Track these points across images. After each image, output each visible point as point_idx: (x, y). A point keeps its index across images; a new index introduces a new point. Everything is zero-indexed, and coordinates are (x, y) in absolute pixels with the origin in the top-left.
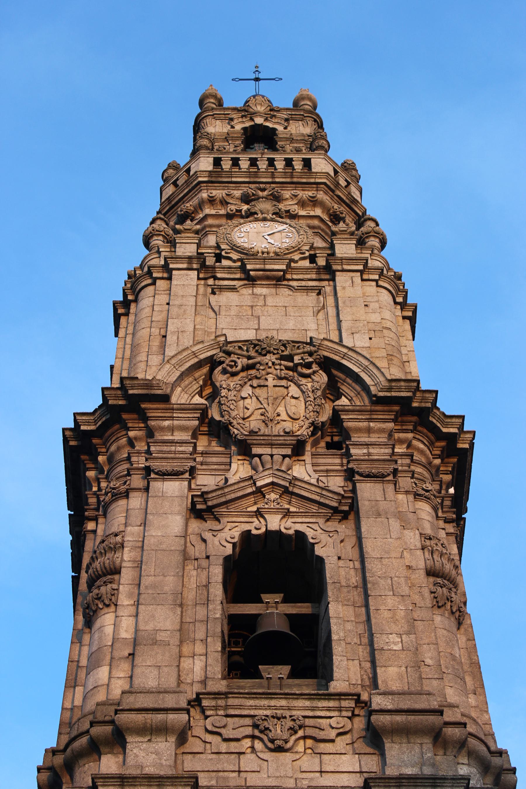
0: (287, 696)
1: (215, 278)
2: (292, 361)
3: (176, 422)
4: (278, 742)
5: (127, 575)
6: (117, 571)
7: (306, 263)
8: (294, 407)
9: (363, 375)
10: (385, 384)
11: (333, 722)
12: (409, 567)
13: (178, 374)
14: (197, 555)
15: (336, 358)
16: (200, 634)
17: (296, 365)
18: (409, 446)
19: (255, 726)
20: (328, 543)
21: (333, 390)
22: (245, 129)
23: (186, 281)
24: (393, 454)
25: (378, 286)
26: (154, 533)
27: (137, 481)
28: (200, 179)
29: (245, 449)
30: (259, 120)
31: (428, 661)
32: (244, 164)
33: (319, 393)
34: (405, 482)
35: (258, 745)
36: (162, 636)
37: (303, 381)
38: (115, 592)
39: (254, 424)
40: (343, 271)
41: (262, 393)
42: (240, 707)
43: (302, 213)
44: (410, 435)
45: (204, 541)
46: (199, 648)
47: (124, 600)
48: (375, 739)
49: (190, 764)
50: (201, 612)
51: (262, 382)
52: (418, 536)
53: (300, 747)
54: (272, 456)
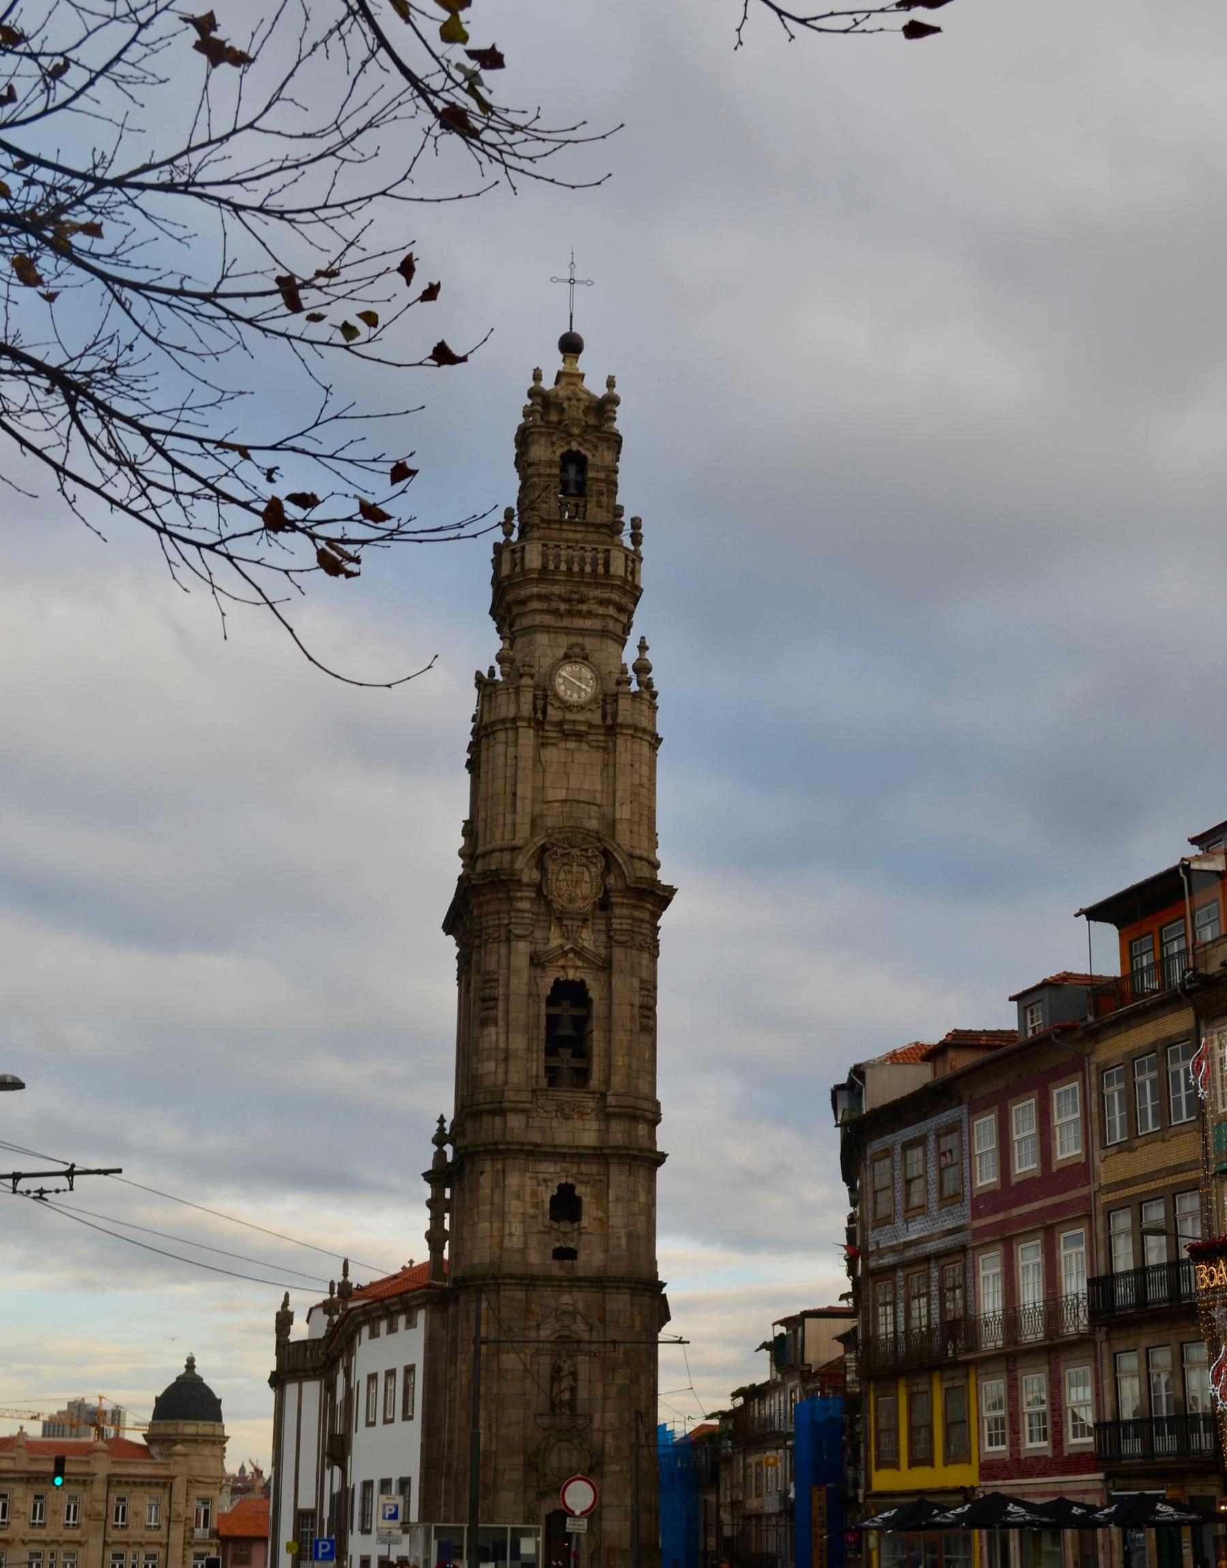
1: (543, 729)
6: (496, 999)
15: (610, 849)
16: (535, 1048)
21: (607, 870)
22: (563, 456)
23: (527, 738)
28: (533, 576)
29: (559, 919)
30: (575, 446)
36: (520, 1053)
41: (569, 877)
43: (601, 611)
46: (535, 1057)
47: (501, 1023)
48: (606, 1116)
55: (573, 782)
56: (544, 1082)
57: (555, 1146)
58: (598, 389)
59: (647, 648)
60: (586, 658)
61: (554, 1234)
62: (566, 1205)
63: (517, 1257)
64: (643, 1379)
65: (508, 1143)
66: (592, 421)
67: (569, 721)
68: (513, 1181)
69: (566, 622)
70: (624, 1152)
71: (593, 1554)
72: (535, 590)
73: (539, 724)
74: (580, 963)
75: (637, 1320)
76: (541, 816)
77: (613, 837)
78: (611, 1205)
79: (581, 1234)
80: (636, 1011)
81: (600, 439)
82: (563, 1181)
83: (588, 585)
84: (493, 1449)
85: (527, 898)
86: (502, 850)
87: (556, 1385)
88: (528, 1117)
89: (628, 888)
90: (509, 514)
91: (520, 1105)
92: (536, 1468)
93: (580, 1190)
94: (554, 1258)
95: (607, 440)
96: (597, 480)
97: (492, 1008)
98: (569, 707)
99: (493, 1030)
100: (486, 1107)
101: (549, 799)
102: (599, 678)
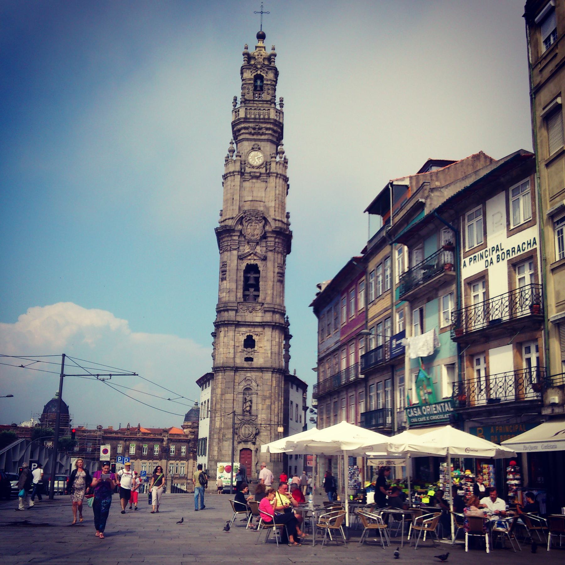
5: (227, 273)
22: (255, 76)
23: (238, 178)
26: (232, 265)
27: (229, 248)
29: (248, 243)
30: (259, 72)
34: (277, 249)
43: (267, 132)
47: (227, 279)
55: (255, 194)
56: (242, 300)
58: (269, 52)
59: (283, 145)
60: (260, 149)
61: (245, 352)
62: (250, 343)
63: (232, 361)
64: (276, 403)
65: (228, 321)
66: (266, 63)
67: (253, 172)
68: (231, 334)
69: (255, 137)
71: (257, 464)
72: (243, 125)
73: (242, 173)
74: (256, 258)
75: (274, 382)
76: (243, 206)
77: (268, 213)
80: (276, 274)
81: (268, 69)
82: (248, 334)
83: (262, 123)
86: (229, 219)
90: (235, 99)
92: (237, 434)
93: (254, 337)
95: (271, 69)
96: (267, 84)
97: (225, 274)
98: (253, 167)
99: (225, 282)
100: (222, 309)
101: (246, 200)
102: (264, 156)
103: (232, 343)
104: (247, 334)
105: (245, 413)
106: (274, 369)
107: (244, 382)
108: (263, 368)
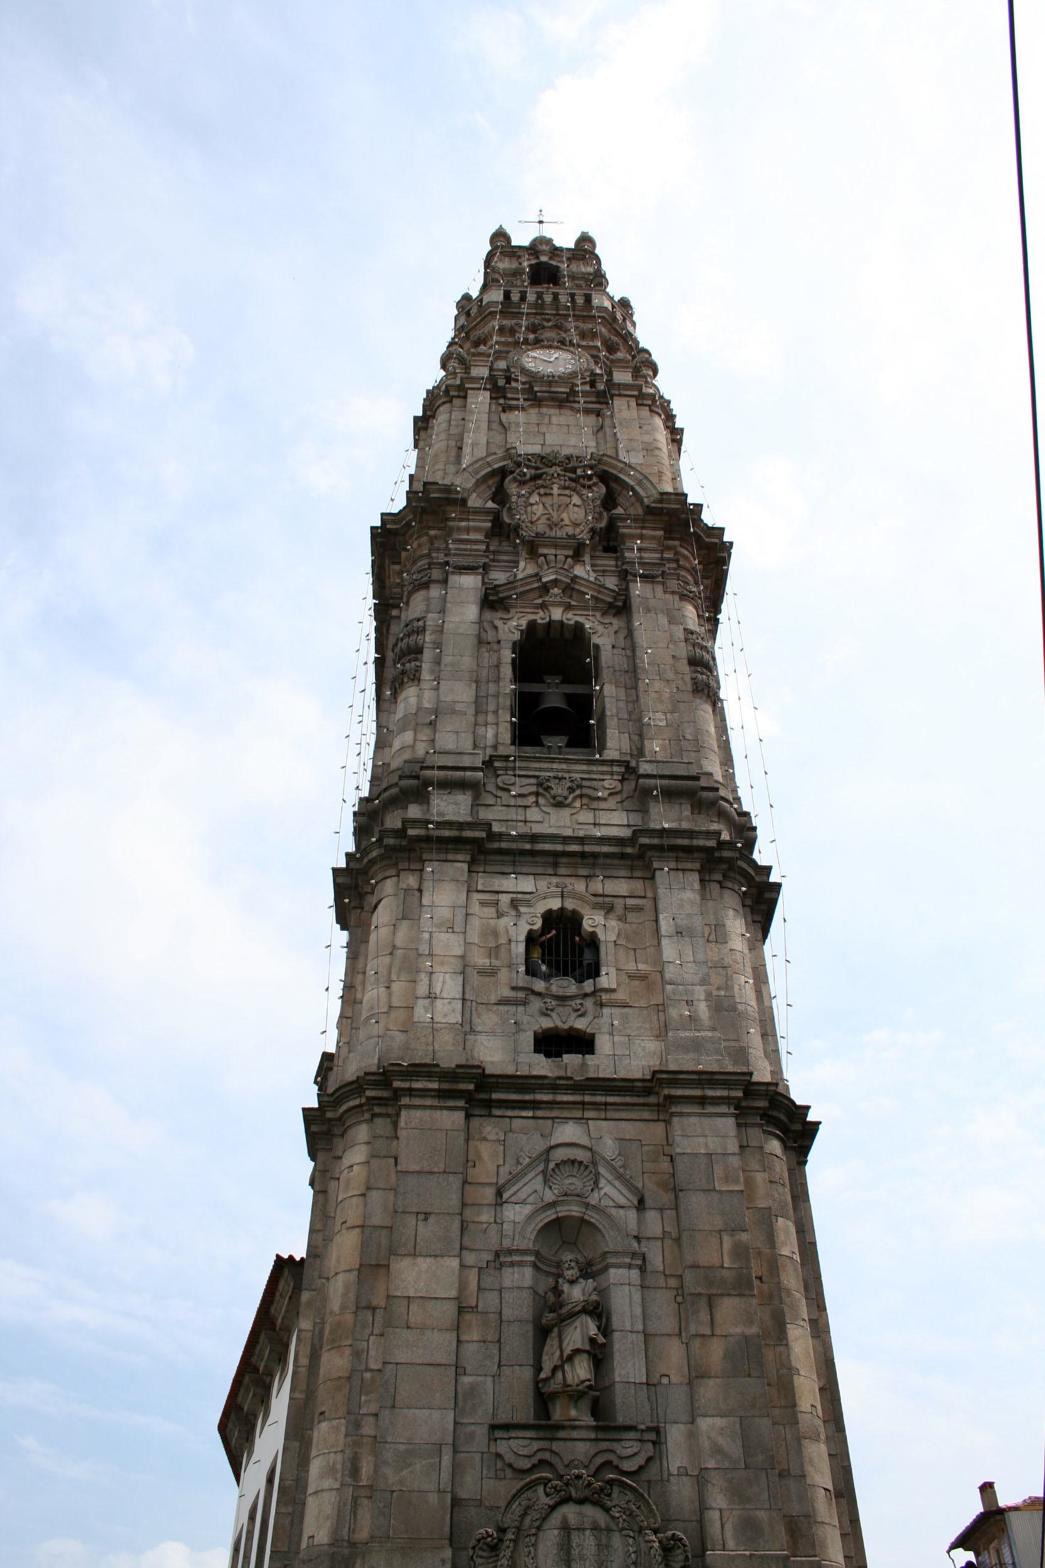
0: (566, 761)
1: (505, 398)
2: (575, 473)
3: (471, 524)
4: (560, 799)
5: (428, 655)
6: (419, 650)
7: (587, 388)
8: (576, 513)
9: (637, 488)
10: (657, 496)
11: (606, 784)
12: (674, 657)
13: (474, 481)
14: (490, 639)
15: (615, 472)
17: (580, 477)
18: (676, 553)
19: (540, 785)
20: (602, 634)
23: (480, 400)
24: (662, 559)
25: (651, 411)
29: (532, 549)
30: (544, 259)
31: (688, 736)
32: (531, 297)
33: (598, 502)
35: (541, 801)
36: (458, 707)
37: (585, 492)
38: (418, 669)
39: (541, 527)
40: (620, 395)
41: (548, 501)
42: (527, 769)
44: (677, 543)
45: (496, 628)
46: (491, 718)
47: (425, 675)
49: (484, 814)
50: (492, 689)
51: (548, 491)
52: (682, 631)
53: (578, 804)
54: (556, 556)
57: (534, 838)
61: (536, 1004)
62: (563, 948)
70: (685, 842)
73: (499, 389)
78: (665, 942)
79: (602, 1005)
82: (555, 904)
84: (363, 1535)
85: (477, 530)
87: (551, 1344)
88: (476, 797)
89: (649, 510)
91: (458, 774)
93: (593, 921)
94: (537, 1050)
103: (449, 944)
104: (542, 907)
105: (558, 1413)
106: (750, 1088)
107: (532, 1188)
108: (675, 1078)
